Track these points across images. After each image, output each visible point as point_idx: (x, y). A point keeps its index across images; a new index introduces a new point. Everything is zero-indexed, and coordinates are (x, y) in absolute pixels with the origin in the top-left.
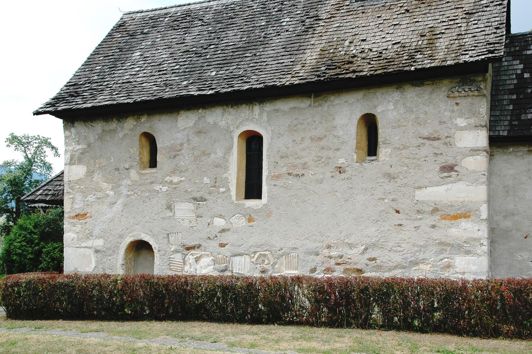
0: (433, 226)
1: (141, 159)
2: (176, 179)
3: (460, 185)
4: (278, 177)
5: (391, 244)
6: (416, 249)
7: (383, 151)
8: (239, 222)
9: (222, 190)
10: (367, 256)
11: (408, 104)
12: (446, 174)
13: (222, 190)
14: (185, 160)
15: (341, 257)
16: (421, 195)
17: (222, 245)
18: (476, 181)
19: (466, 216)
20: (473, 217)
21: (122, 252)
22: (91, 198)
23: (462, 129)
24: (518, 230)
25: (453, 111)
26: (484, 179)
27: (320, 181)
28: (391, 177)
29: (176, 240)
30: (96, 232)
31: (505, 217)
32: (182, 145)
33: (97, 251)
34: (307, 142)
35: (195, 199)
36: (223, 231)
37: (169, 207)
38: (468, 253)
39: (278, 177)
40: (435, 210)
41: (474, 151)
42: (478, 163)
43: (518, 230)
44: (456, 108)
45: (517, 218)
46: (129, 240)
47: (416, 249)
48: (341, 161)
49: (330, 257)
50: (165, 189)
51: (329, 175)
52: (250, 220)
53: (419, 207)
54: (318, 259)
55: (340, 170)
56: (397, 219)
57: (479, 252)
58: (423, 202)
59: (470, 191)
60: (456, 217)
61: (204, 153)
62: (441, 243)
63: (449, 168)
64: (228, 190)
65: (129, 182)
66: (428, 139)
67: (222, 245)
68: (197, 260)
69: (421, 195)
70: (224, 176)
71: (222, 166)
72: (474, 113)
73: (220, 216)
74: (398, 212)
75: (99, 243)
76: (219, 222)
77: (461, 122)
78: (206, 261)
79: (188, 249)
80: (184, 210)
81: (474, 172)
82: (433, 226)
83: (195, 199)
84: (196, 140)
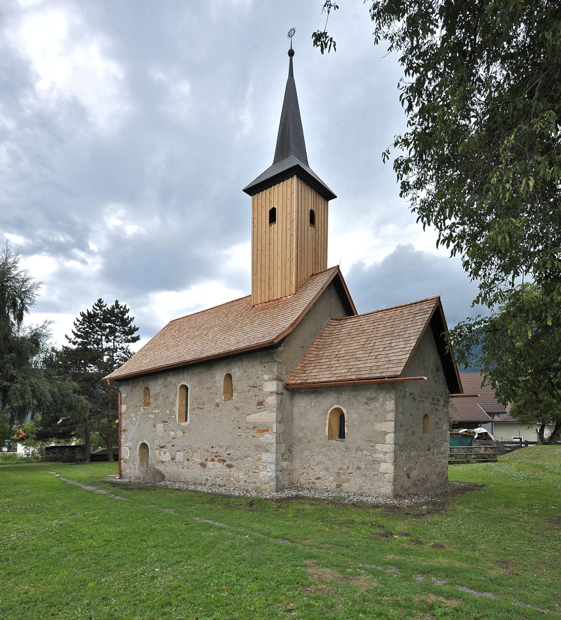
0: (254, 436)
1: (145, 401)
2: (157, 411)
3: (265, 413)
4: (194, 409)
5: (237, 446)
6: (246, 449)
7: (235, 394)
8: (180, 433)
9: (173, 417)
10: (227, 452)
11: (244, 367)
12: (259, 407)
13: (173, 417)
14: (160, 402)
15: (217, 453)
16: (250, 418)
17: (173, 446)
18: (271, 411)
19: (267, 431)
20: (270, 431)
21: (138, 449)
22: (128, 422)
23: (266, 381)
24: (306, 438)
25: (262, 371)
26: (275, 409)
27: (210, 412)
28: (237, 409)
29: (157, 442)
30: (129, 439)
31: (300, 430)
32: (159, 393)
33: (130, 448)
34: (205, 390)
35: (163, 422)
36: (174, 438)
37: (154, 426)
38: (267, 451)
39: (194, 409)
40: (255, 427)
41: (271, 393)
42: (272, 400)
43: (306, 438)
44: (264, 369)
45: (305, 431)
46: (140, 443)
47: (246, 449)
48: (218, 400)
49: (213, 453)
50: (152, 416)
51: (213, 408)
52: (184, 433)
53: (248, 425)
54: (208, 454)
55: (217, 405)
56: (239, 432)
57: (272, 451)
58: (250, 423)
59: (269, 417)
60: (263, 431)
61: (167, 398)
62: (257, 446)
63: (260, 403)
64: (175, 417)
65: (140, 413)
66: (252, 387)
67: (173, 446)
68: (165, 453)
69: (250, 418)
70: (174, 409)
71: (173, 404)
72: (271, 372)
73: (173, 431)
74: (239, 428)
75: (130, 444)
76: (172, 433)
77: (266, 377)
78: (167, 453)
79: (161, 448)
80: (160, 426)
81: (271, 405)
82: (254, 436)
83: (163, 422)
84: (164, 390)
